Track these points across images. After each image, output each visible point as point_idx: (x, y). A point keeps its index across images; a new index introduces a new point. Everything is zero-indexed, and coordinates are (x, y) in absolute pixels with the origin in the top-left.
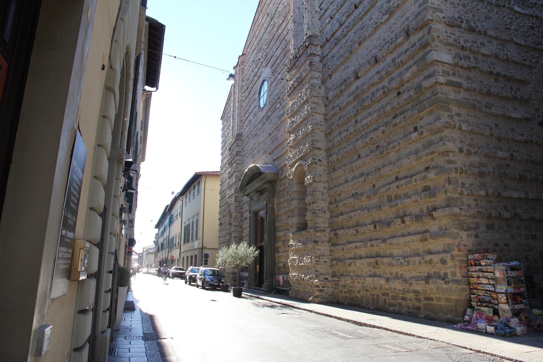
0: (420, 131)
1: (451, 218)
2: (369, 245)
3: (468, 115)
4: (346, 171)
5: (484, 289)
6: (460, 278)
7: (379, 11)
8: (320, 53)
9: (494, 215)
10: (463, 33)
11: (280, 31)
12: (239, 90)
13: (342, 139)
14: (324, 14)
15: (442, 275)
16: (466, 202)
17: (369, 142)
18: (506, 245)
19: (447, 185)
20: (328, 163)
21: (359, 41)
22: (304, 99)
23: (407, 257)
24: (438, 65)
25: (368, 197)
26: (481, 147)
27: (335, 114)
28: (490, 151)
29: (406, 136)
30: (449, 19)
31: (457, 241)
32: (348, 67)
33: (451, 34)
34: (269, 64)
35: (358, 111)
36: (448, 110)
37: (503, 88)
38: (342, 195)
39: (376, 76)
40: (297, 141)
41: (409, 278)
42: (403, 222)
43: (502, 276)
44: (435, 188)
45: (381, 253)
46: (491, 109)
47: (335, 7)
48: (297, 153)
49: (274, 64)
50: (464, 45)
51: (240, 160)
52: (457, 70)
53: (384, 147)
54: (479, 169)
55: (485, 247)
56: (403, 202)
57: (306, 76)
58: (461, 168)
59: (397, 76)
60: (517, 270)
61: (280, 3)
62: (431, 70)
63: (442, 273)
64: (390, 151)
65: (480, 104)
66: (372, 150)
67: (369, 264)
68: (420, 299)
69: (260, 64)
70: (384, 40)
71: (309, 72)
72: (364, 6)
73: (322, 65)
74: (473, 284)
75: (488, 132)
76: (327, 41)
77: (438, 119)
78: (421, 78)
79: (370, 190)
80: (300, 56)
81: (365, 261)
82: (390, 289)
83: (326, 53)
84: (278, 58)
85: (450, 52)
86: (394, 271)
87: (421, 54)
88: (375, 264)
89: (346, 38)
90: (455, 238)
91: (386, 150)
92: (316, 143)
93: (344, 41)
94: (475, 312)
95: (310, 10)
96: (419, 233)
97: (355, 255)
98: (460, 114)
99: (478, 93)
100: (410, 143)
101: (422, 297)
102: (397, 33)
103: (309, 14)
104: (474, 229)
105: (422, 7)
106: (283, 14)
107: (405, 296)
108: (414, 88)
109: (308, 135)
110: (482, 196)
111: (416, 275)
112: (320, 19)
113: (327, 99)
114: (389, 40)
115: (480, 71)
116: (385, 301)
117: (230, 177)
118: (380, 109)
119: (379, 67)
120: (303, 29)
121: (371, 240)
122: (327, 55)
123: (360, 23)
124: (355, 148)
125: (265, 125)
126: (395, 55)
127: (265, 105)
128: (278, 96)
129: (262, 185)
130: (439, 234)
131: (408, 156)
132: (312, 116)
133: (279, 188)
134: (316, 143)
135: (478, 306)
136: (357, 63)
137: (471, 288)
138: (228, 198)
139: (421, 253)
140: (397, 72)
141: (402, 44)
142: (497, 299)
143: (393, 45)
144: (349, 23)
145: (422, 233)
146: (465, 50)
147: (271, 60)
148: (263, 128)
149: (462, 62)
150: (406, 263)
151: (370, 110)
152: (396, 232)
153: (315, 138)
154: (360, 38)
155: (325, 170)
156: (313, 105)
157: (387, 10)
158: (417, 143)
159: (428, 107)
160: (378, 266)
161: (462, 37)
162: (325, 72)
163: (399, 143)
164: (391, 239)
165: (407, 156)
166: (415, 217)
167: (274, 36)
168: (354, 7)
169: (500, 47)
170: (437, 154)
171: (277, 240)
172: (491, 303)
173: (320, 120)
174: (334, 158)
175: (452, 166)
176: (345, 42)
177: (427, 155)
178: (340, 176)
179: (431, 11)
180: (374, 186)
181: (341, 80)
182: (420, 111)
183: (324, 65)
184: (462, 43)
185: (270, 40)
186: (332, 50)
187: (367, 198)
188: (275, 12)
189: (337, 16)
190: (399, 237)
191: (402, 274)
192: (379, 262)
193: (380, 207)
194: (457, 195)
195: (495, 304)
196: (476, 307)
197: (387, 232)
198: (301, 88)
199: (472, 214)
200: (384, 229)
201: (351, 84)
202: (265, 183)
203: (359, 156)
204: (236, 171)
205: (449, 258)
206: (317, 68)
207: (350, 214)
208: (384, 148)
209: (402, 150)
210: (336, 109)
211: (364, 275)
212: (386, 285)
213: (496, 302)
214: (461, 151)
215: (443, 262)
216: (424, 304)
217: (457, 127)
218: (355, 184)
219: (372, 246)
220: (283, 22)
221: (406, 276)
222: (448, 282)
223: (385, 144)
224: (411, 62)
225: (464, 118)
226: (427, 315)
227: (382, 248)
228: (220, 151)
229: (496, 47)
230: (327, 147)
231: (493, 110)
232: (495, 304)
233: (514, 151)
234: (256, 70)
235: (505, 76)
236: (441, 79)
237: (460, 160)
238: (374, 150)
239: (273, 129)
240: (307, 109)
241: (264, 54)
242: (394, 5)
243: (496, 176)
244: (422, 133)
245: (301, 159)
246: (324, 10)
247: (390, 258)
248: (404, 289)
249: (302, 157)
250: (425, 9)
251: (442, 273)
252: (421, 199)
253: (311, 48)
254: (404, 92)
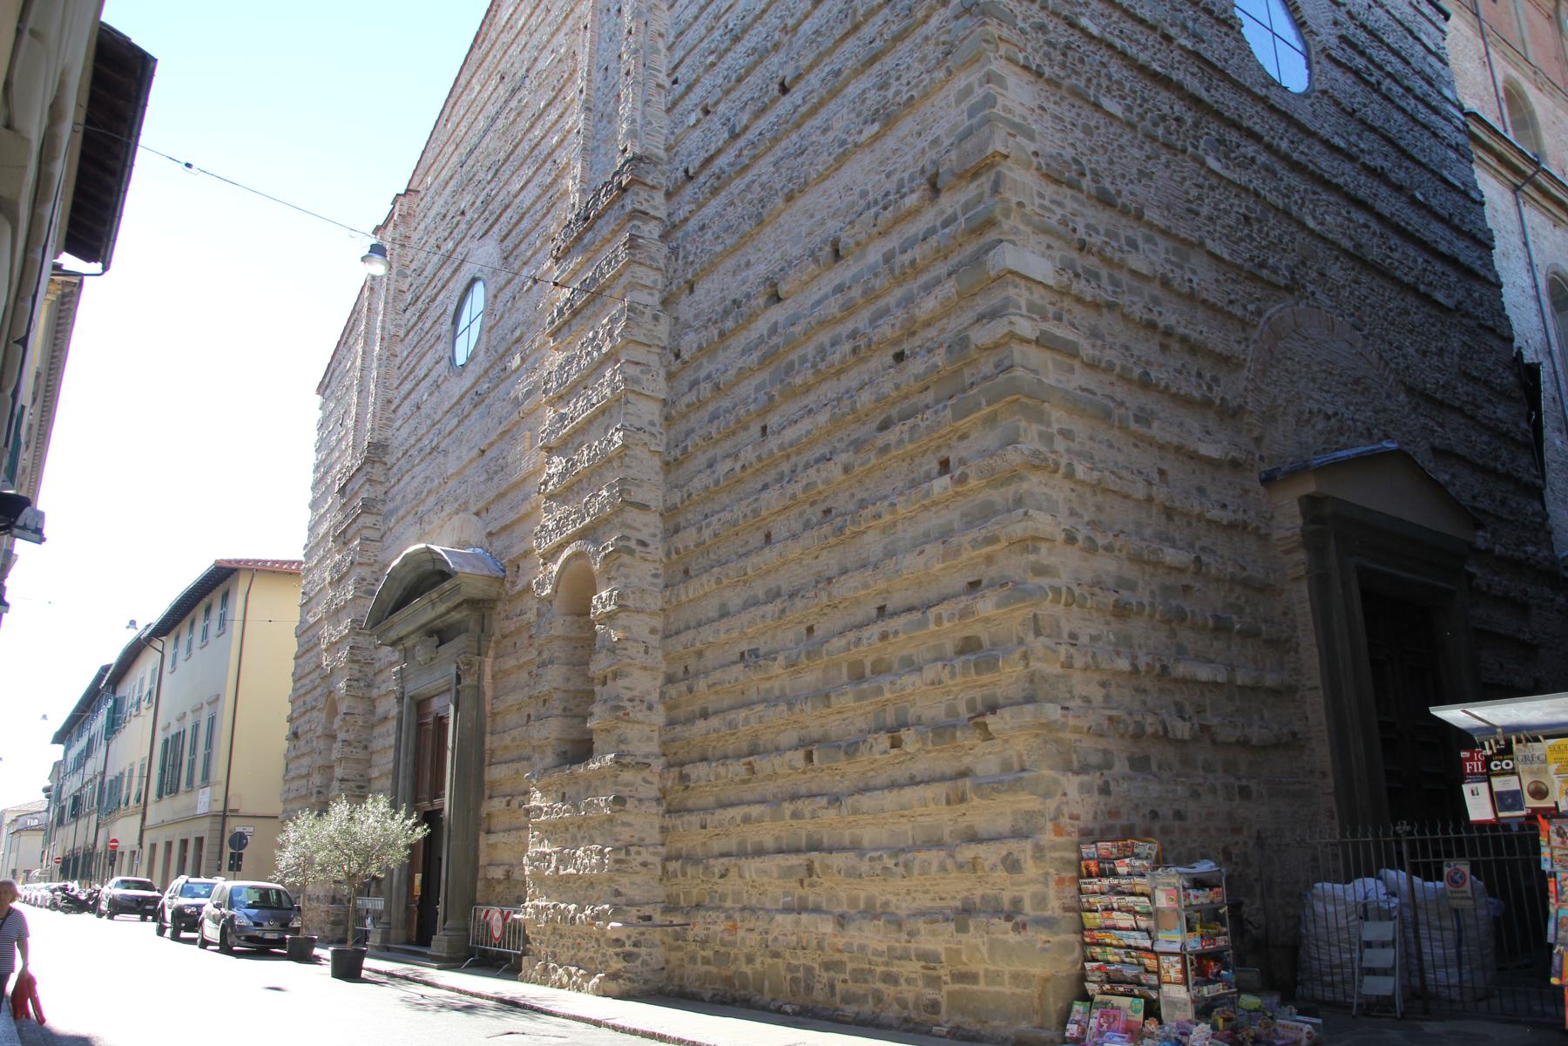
0: (957, 473)
1: (1037, 735)
2: (788, 813)
3: (1092, 438)
4: (725, 581)
5: (1122, 943)
6: (1059, 913)
7: (854, 109)
8: (662, 213)
9: (1150, 730)
10: (1083, 204)
11: (537, 132)
12: (386, 303)
13: (717, 483)
14: (682, 97)
15: (1007, 906)
16: (1079, 689)
17: (800, 496)
18: (1179, 815)
19: (1030, 637)
20: (668, 554)
21: (786, 190)
22: (604, 350)
23: (903, 850)
24: (1016, 286)
25: (791, 664)
26: (1122, 532)
27: (700, 404)
28: (1144, 544)
29: (914, 484)
30: (1049, 160)
31: (1052, 805)
32: (748, 264)
33: (1053, 202)
34: (496, 228)
35: (771, 398)
36: (1041, 417)
37: (1180, 372)
38: (708, 653)
39: (832, 299)
40: (574, 479)
41: (909, 916)
42: (896, 744)
43: (1173, 904)
44: (994, 645)
45: (825, 841)
46: (1149, 426)
47: (719, 81)
48: (570, 515)
49: (511, 231)
50: (1087, 238)
51: (374, 527)
52: (1065, 305)
53: (846, 514)
54: (1116, 596)
55: (1123, 821)
56: (899, 682)
57: (614, 278)
58: (1069, 588)
59: (898, 305)
60: (1211, 888)
61: (544, 47)
62: (996, 298)
63: (1006, 897)
64: (863, 526)
65: (1123, 411)
66: (808, 520)
67: (787, 873)
68: (939, 977)
69: (463, 226)
70: (864, 194)
71: (627, 264)
72: (809, 88)
73: (665, 250)
74: (1091, 930)
75: (1140, 491)
76: (689, 178)
77: (1012, 440)
78: (968, 316)
79: (797, 644)
80: (599, 216)
81: (774, 863)
82: (848, 948)
83: (682, 214)
84: (524, 214)
85: (1048, 252)
86: (862, 895)
87: (969, 249)
88: (803, 873)
89: (749, 177)
90: (1047, 795)
91: (853, 522)
92: (633, 489)
93: (738, 185)
94: (1096, 1013)
95: (640, 79)
96: (942, 778)
97: (742, 844)
98: (1071, 431)
99: (1121, 377)
100: (926, 508)
101: (944, 973)
102: (902, 179)
103: (639, 90)
104: (1099, 768)
105: (979, 117)
106: (553, 80)
107: (894, 969)
108: (946, 345)
109: (610, 461)
110: (1117, 673)
111: (930, 904)
112: (668, 110)
113: (677, 356)
114: (879, 198)
115: (1124, 316)
116: (832, 987)
117: (339, 580)
118: (839, 399)
119: (843, 273)
120: (615, 133)
121: (794, 797)
122: (686, 220)
123: (794, 137)
124: (756, 512)
125: (466, 422)
126: (893, 242)
127: (471, 358)
128: (517, 333)
129: (448, 612)
130: (1001, 782)
131: (918, 545)
132: (627, 402)
133: (499, 626)
134: (633, 489)
135: (1104, 993)
136: (778, 255)
137: (1088, 940)
138: (326, 650)
139: (947, 838)
140: (898, 293)
141: (914, 213)
142: (1158, 973)
143: (888, 214)
144: (760, 134)
145: (951, 779)
146: (1089, 252)
147: (503, 219)
148: (461, 429)
149: (1079, 286)
150: (901, 869)
151: (810, 400)
152: (872, 773)
153: (631, 473)
154: (790, 180)
155: (655, 576)
156: (632, 371)
157: (877, 111)
158: (947, 506)
159: (984, 403)
160: (815, 878)
161: (1082, 215)
162: (675, 271)
163: (893, 505)
164: (856, 797)
165: (916, 547)
166: (933, 730)
167: (516, 146)
168: (777, 87)
169: (1173, 259)
170: (1004, 543)
171: (487, 792)
172: (1139, 984)
173: (650, 417)
174: (688, 538)
175: (1045, 581)
176: (742, 187)
177: (975, 544)
178: (705, 594)
179: (1001, 132)
180: (810, 630)
181: (723, 299)
182: (960, 414)
183: (674, 251)
184: (1081, 231)
185: (502, 155)
186: (700, 206)
187: (787, 667)
188: (527, 71)
189: (722, 108)
190: (882, 789)
191: (886, 904)
192: (816, 865)
193: (827, 696)
194: (1057, 669)
195: (1151, 987)
196: (1098, 998)
197: (849, 771)
198: (596, 315)
199: (1093, 724)
200: (835, 765)
201: (753, 316)
203: (768, 536)
204: (360, 564)
205: (1029, 853)
206: (652, 259)
207: (732, 716)
208: (848, 518)
209: (900, 527)
210: (703, 385)
211: (768, 905)
212: (836, 936)
213: (1153, 980)
214: (1071, 539)
215: (1012, 865)
216: (950, 994)
217: (1062, 470)
218: (752, 623)
219: (795, 815)
220: (549, 105)
221: (897, 908)
222: (1024, 926)
223: (851, 507)
224: (941, 269)
225: (1082, 444)
226: (958, 1027)
227: (827, 822)
228: (309, 496)
229: (1163, 256)
230: (669, 504)
231: (1156, 431)
232: (1151, 987)
233: (1203, 549)
234: (450, 245)
235: (1184, 339)
236: (1025, 328)
237: (1068, 565)
238: (814, 520)
239: (493, 437)
240: (612, 380)
241: (481, 198)
242: (898, 99)
243: (1158, 616)
244: (963, 479)
245: (582, 535)
246: (683, 86)
247: (852, 855)
248: (890, 949)
249: (585, 529)
250: (987, 121)
251: (1006, 897)
252: (953, 675)
253: (637, 194)
254: (914, 354)
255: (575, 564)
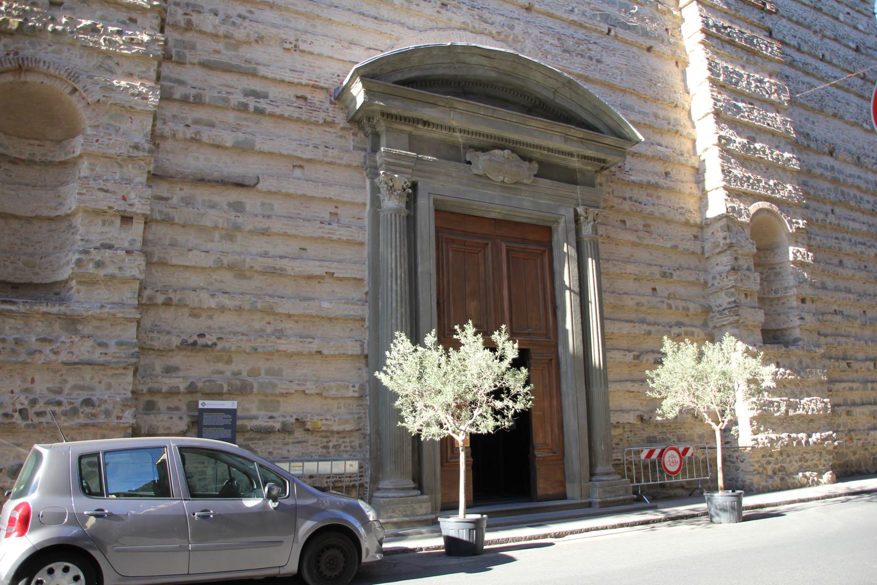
97: (845, 400)
129: (571, 154)
202: (584, 157)
211: (861, 428)
218: (844, 299)
255: (765, 215)
